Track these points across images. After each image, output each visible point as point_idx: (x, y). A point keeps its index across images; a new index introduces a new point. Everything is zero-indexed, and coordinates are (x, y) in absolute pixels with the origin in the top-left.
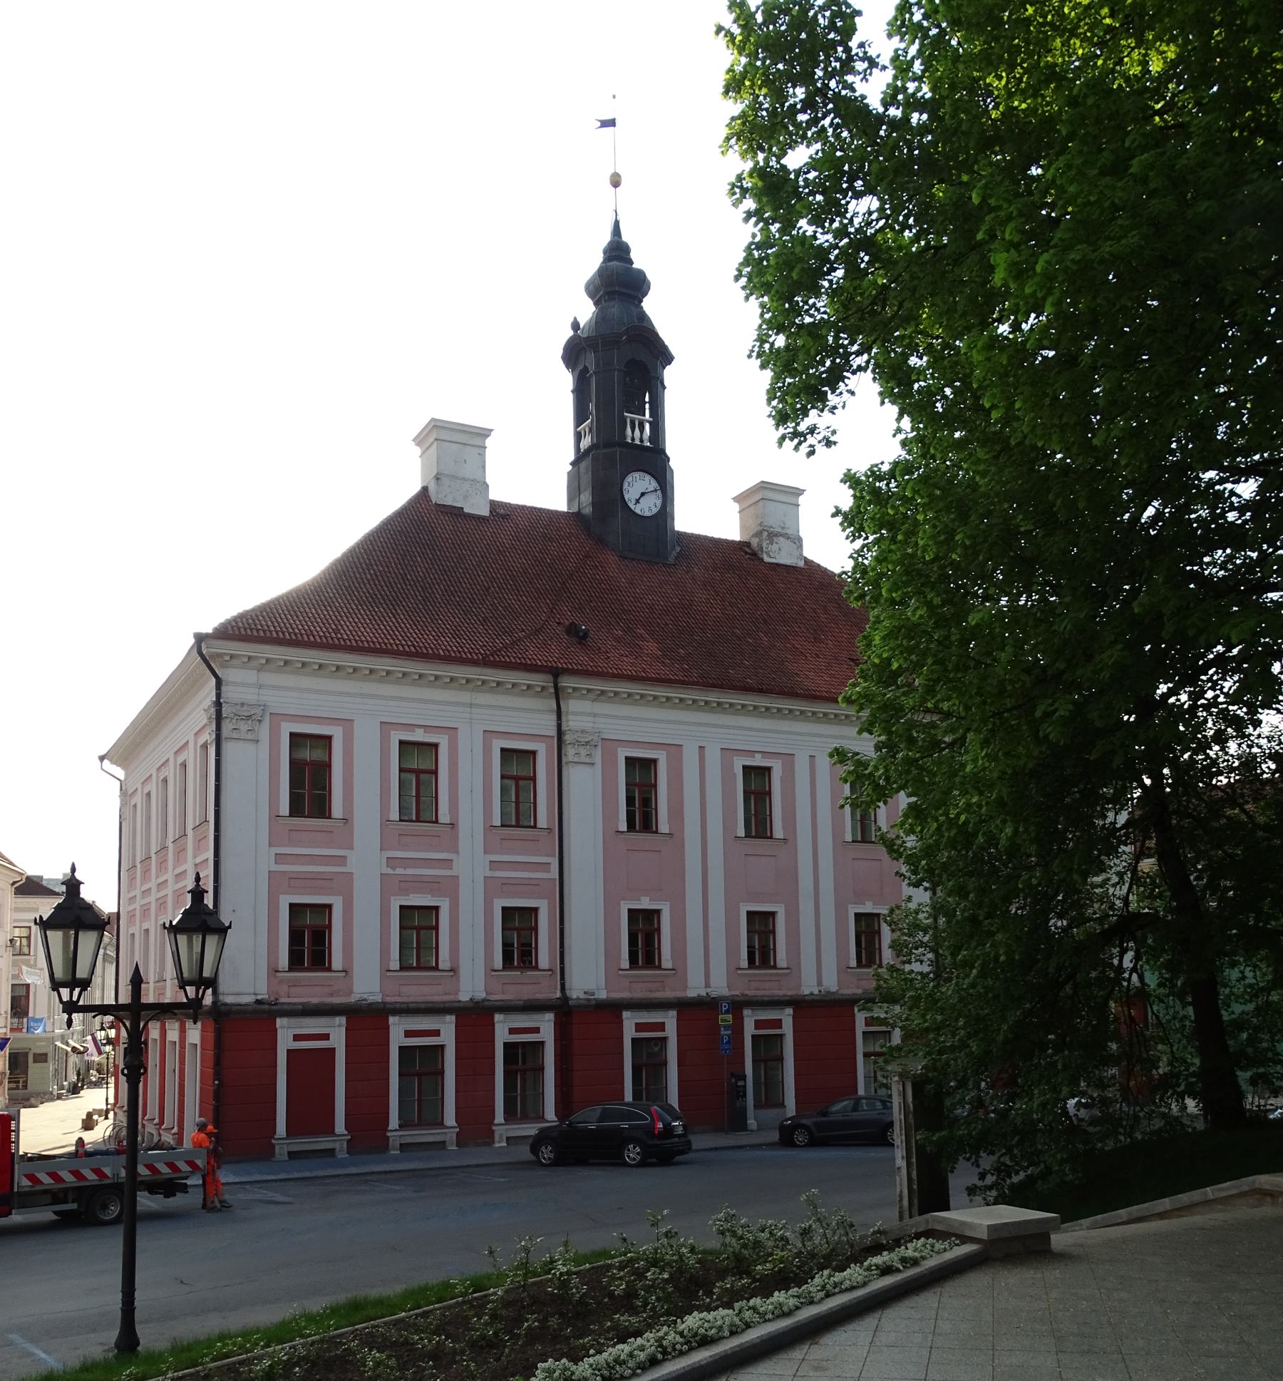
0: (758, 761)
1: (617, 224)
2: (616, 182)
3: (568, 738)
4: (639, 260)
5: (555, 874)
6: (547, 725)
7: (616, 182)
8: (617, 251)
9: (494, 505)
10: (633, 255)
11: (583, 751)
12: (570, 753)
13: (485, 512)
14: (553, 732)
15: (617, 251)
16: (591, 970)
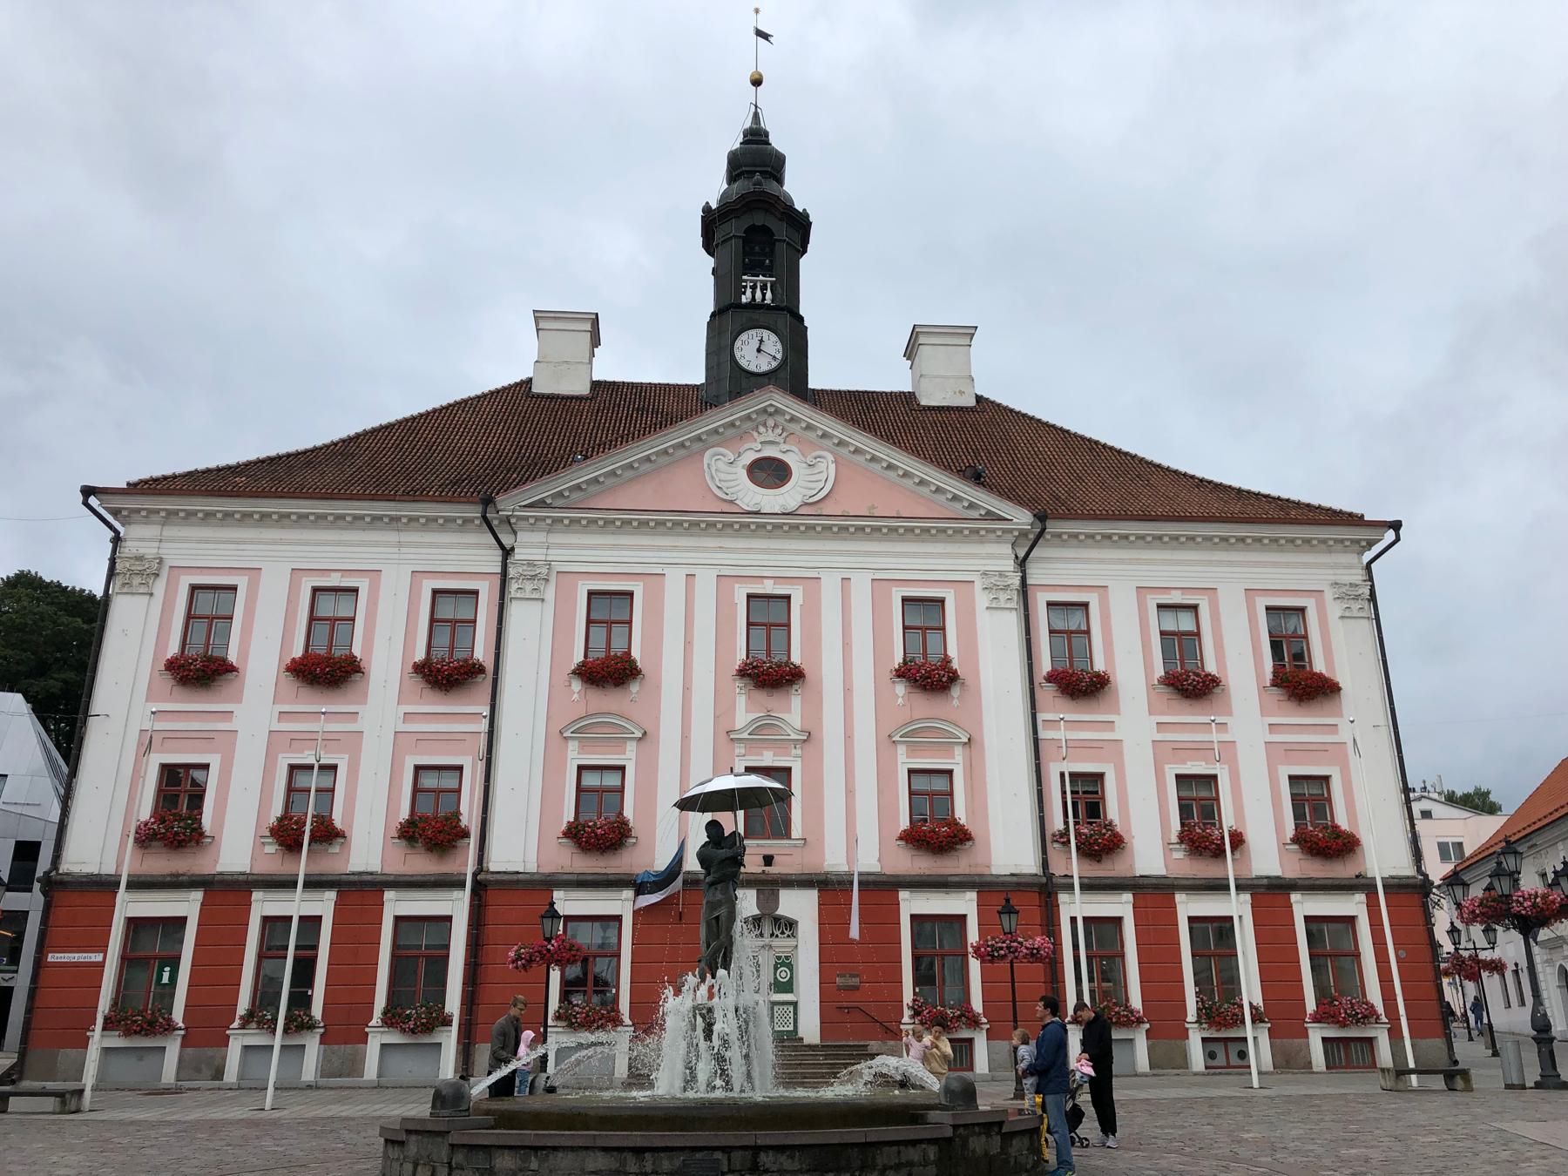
0: (768, 588)
1: (756, 115)
2: (757, 82)
3: (512, 572)
4: (777, 142)
5: (483, 726)
6: (491, 561)
7: (757, 82)
8: (756, 137)
9: (597, 385)
10: (772, 139)
11: (529, 586)
12: (513, 587)
13: (583, 389)
14: (499, 570)
15: (756, 137)
16: (520, 839)
